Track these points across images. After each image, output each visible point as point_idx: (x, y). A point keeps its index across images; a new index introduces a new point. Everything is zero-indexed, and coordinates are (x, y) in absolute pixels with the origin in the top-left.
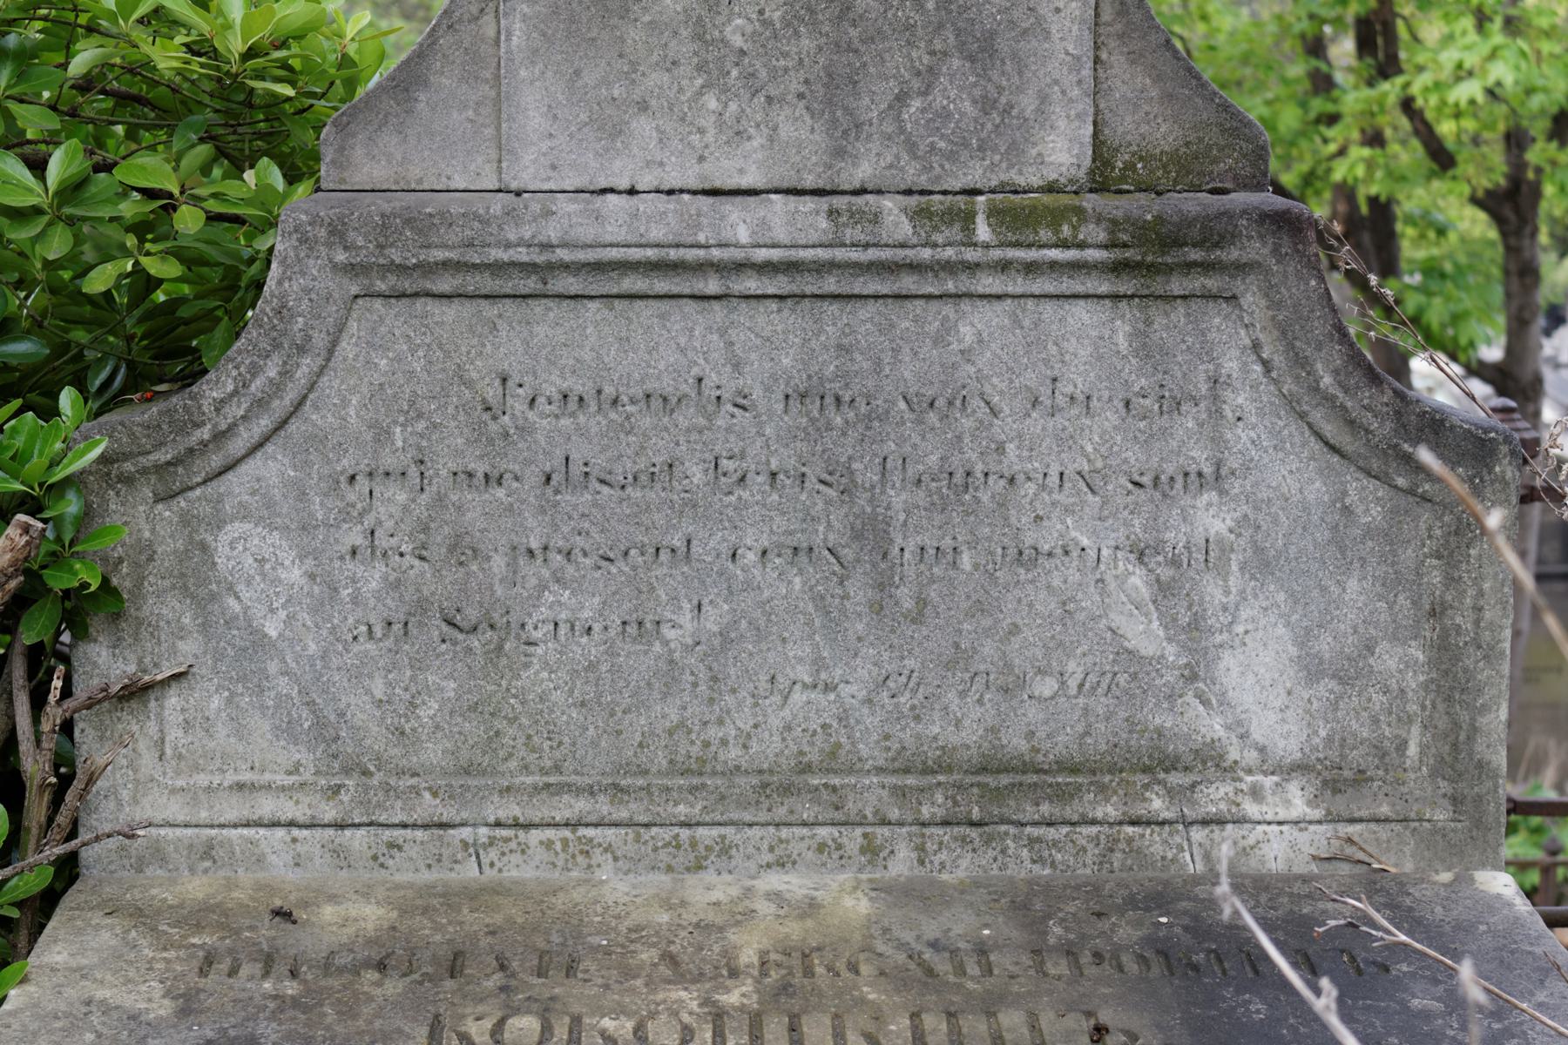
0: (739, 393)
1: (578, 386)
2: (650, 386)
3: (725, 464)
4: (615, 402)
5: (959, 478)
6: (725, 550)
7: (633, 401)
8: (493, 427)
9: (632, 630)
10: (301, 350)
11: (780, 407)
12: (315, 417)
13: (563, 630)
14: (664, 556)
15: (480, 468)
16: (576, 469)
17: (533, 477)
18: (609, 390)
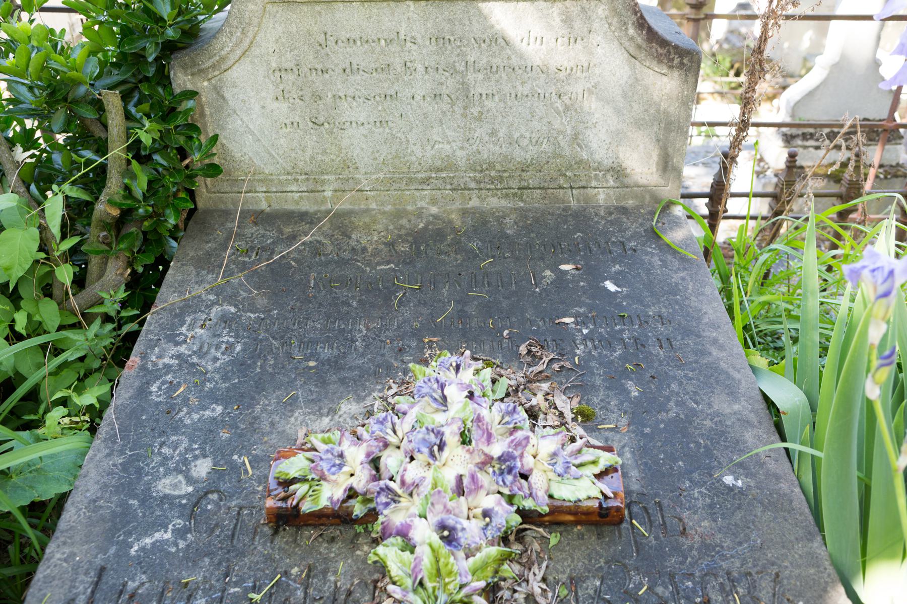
0: (412, 37)
1: (355, 35)
2: (380, 36)
3: (408, 64)
4: (367, 41)
5: (494, 69)
6: (409, 95)
7: (373, 41)
8: (323, 52)
9: (378, 124)
10: (249, 24)
11: (428, 42)
12: (256, 51)
13: (354, 124)
14: (388, 98)
15: (319, 67)
16: (355, 67)
17: (339, 70)
18: (364, 37)
